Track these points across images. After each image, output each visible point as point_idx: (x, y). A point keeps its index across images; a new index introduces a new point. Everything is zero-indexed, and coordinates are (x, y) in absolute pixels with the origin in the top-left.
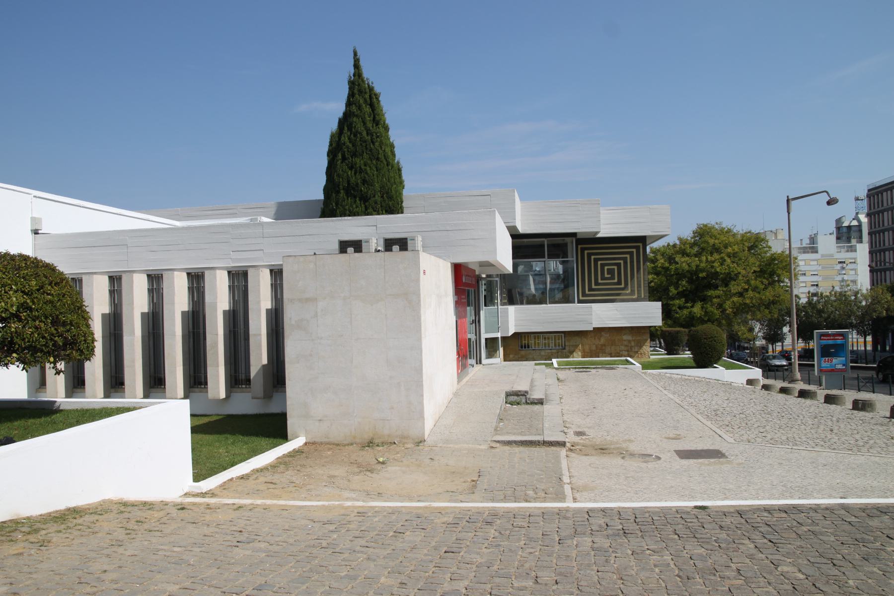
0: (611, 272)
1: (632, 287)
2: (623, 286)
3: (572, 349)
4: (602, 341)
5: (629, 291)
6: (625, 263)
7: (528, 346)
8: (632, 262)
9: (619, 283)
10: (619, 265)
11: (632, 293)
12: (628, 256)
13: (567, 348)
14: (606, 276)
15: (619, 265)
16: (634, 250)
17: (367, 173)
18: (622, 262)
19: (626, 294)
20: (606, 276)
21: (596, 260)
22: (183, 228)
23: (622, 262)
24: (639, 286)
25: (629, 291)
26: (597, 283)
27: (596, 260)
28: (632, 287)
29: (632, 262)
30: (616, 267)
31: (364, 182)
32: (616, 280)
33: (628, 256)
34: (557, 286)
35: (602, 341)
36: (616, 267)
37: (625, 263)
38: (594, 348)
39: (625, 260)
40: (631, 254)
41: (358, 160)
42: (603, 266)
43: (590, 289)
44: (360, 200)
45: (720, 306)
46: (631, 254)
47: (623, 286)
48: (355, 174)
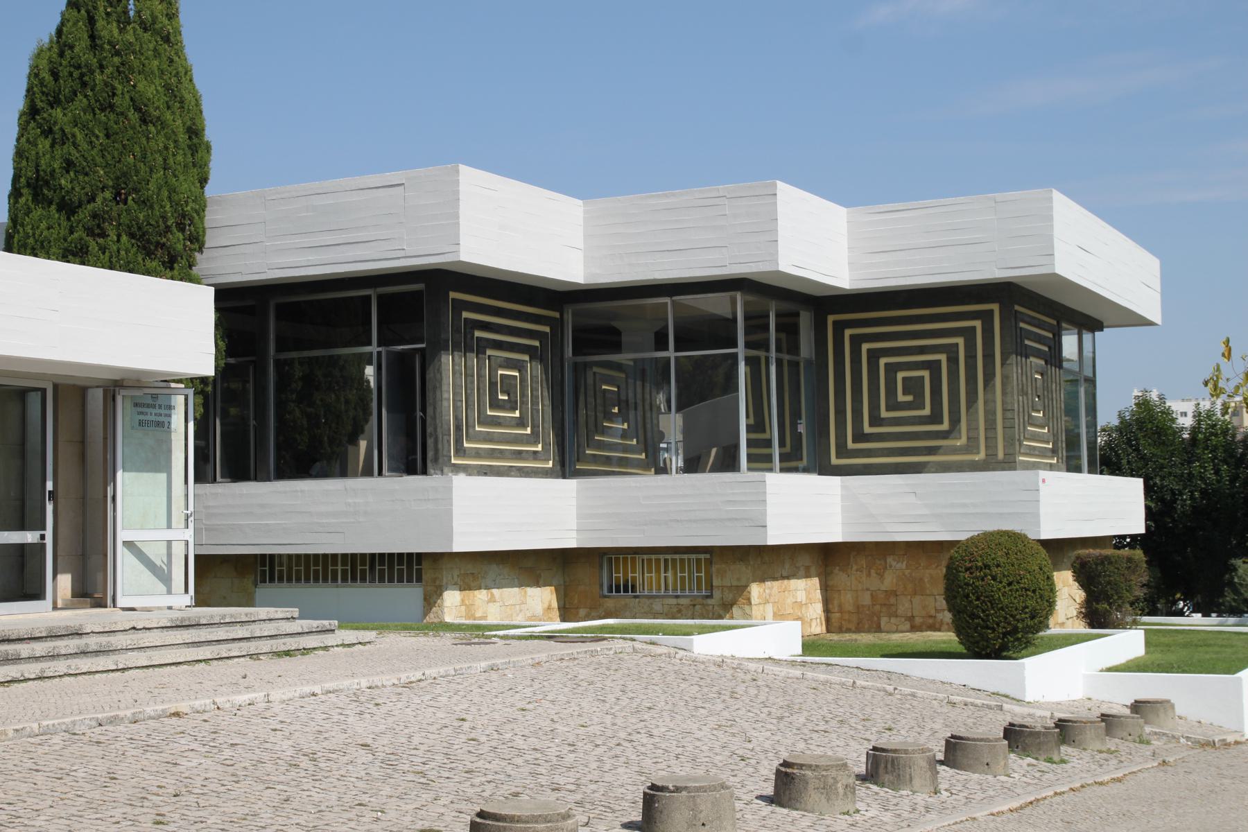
0: (913, 386)
1: (972, 428)
2: (945, 426)
3: (729, 596)
4: (889, 581)
5: (962, 441)
6: (953, 361)
7: (628, 587)
8: (971, 357)
9: (936, 418)
10: (934, 367)
11: (971, 446)
12: (960, 341)
13: (717, 594)
14: (901, 398)
15: (934, 367)
16: (978, 324)
17: (75, 145)
18: (943, 357)
19: (955, 450)
20: (901, 398)
21: (874, 356)
22: (337, 346)
23: (943, 357)
24: (990, 426)
25: (962, 441)
26: (876, 420)
27: (874, 356)
28: (972, 428)
29: (971, 357)
30: (926, 374)
31: (69, 165)
32: (927, 411)
33: (960, 341)
34: (672, 425)
35: (889, 581)
36: (926, 374)
37: (953, 361)
38: (866, 600)
39: (951, 351)
40: (969, 334)
41: (58, 113)
42: (892, 369)
43: (860, 437)
44: (59, 210)
45: (1202, 479)
46: (969, 334)
47: (945, 426)
48: (52, 146)
